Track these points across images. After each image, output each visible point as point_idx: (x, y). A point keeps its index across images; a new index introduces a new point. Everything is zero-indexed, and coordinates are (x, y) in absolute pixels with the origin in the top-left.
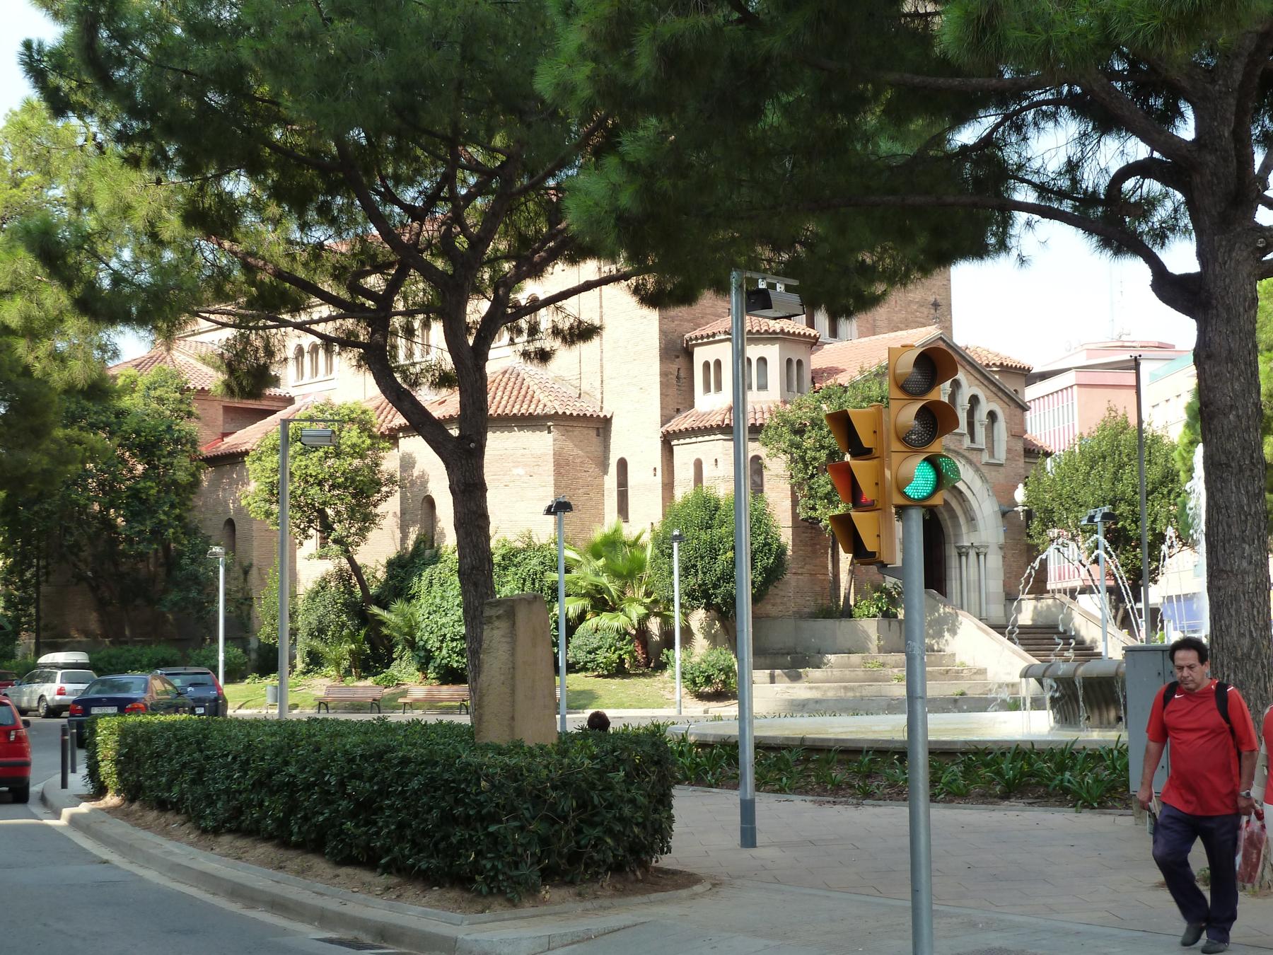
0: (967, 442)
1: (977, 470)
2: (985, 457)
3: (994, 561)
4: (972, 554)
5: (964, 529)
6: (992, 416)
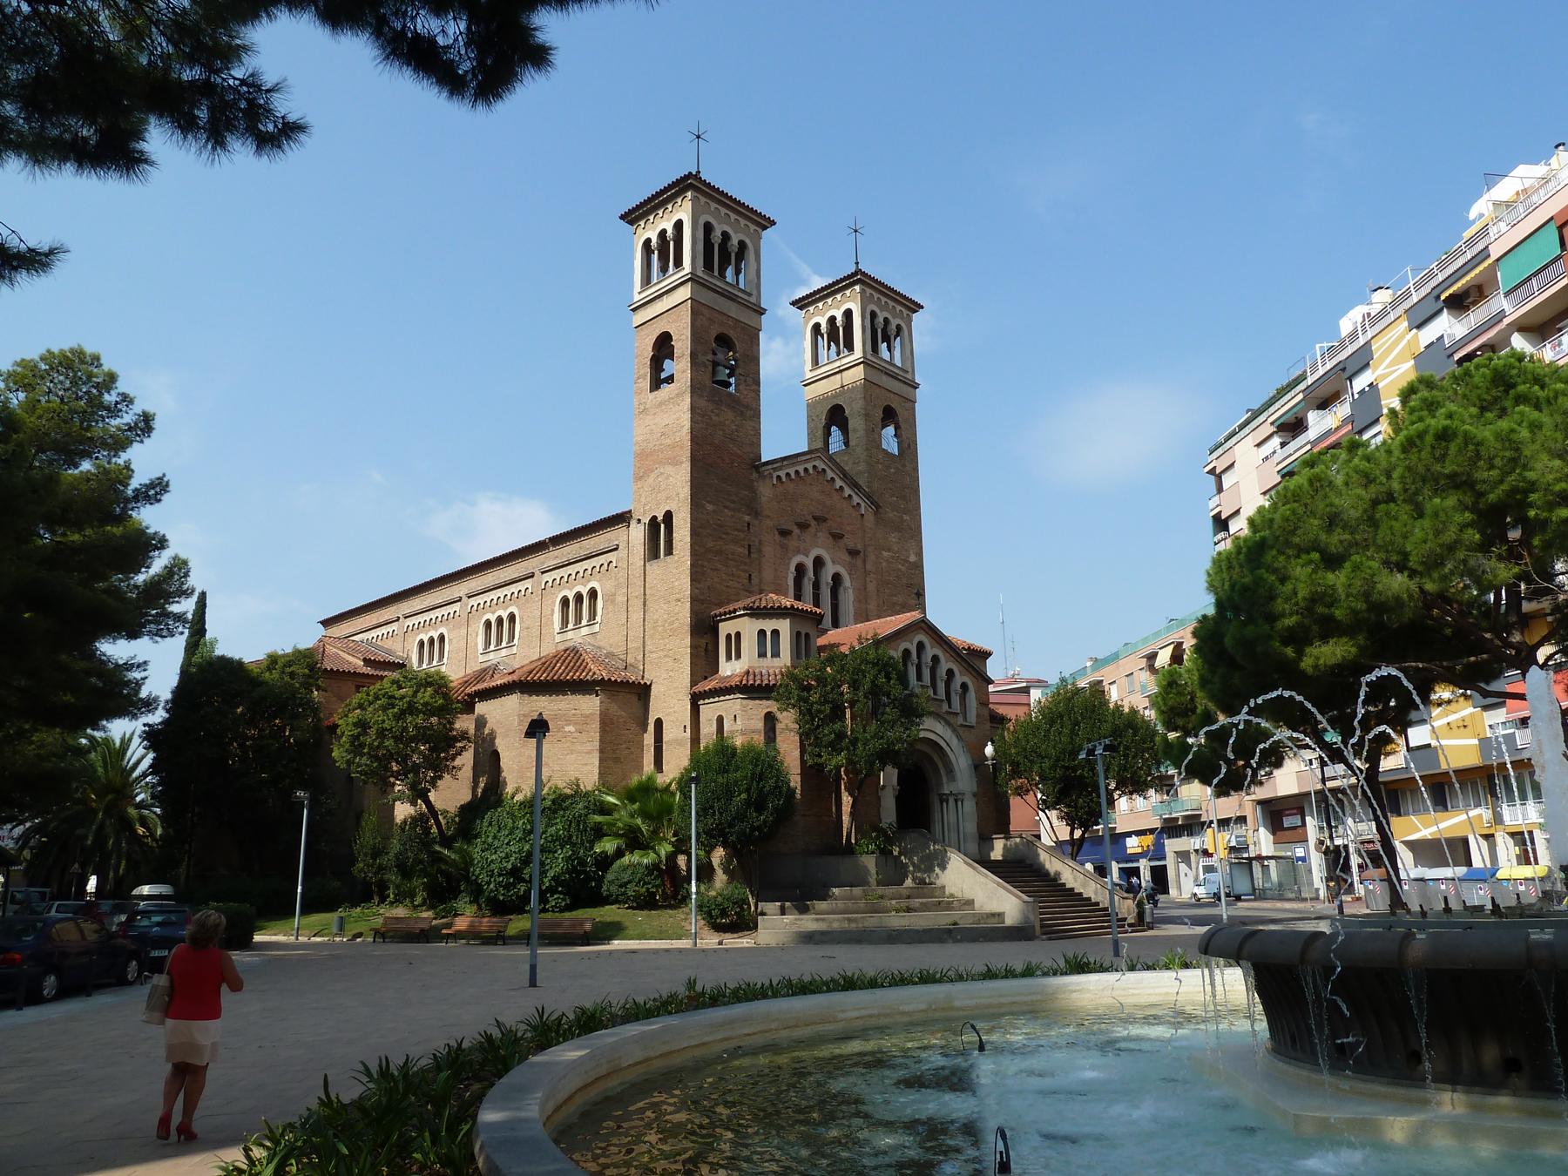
0: (945, 707)
1: (954, 730)
2: (960, 720)
3: (969, 806)
4: (951, 800)
5: (944, 779)
6: (964, 686)
